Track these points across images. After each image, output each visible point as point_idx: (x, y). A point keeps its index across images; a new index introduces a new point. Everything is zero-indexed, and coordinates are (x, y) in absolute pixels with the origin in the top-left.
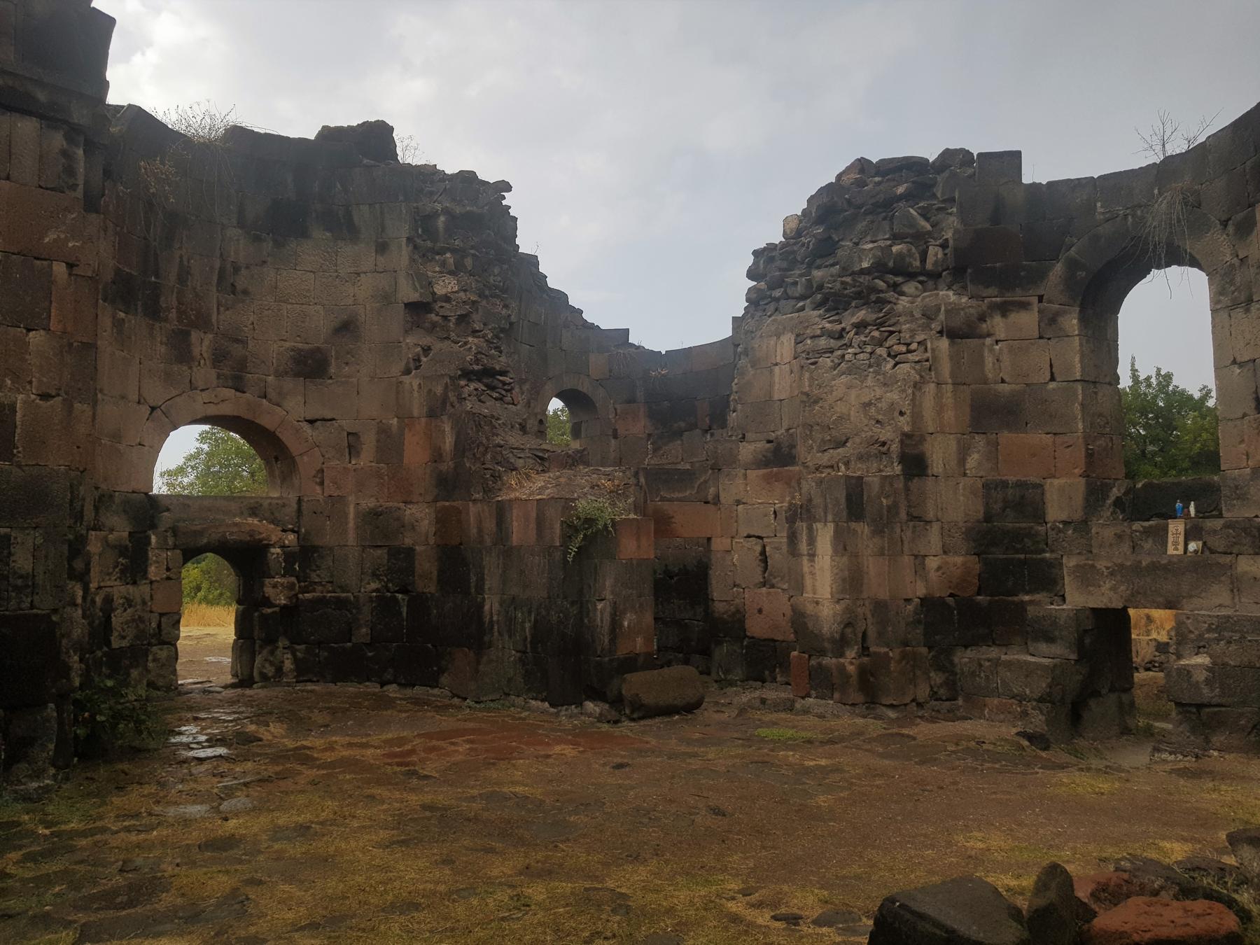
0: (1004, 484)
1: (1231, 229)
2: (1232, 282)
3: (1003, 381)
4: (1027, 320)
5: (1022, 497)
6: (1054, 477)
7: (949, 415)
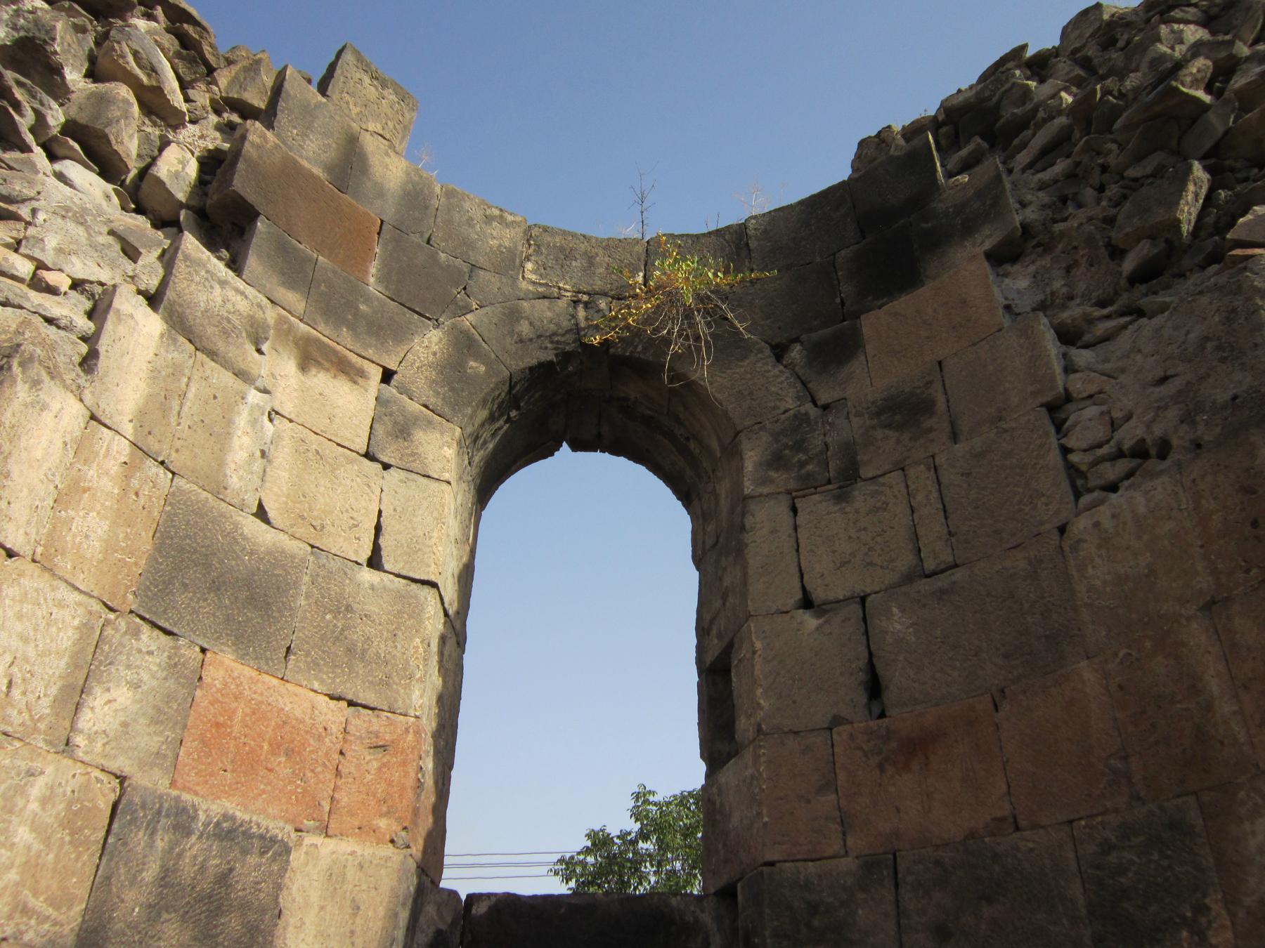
0: (182, 820)
1: (796, 353)
2: (798, 446)
3: (261, 513)
4: (351, 405)
5: (224, 879)
6: (325, 831)
7: (91, 528)
